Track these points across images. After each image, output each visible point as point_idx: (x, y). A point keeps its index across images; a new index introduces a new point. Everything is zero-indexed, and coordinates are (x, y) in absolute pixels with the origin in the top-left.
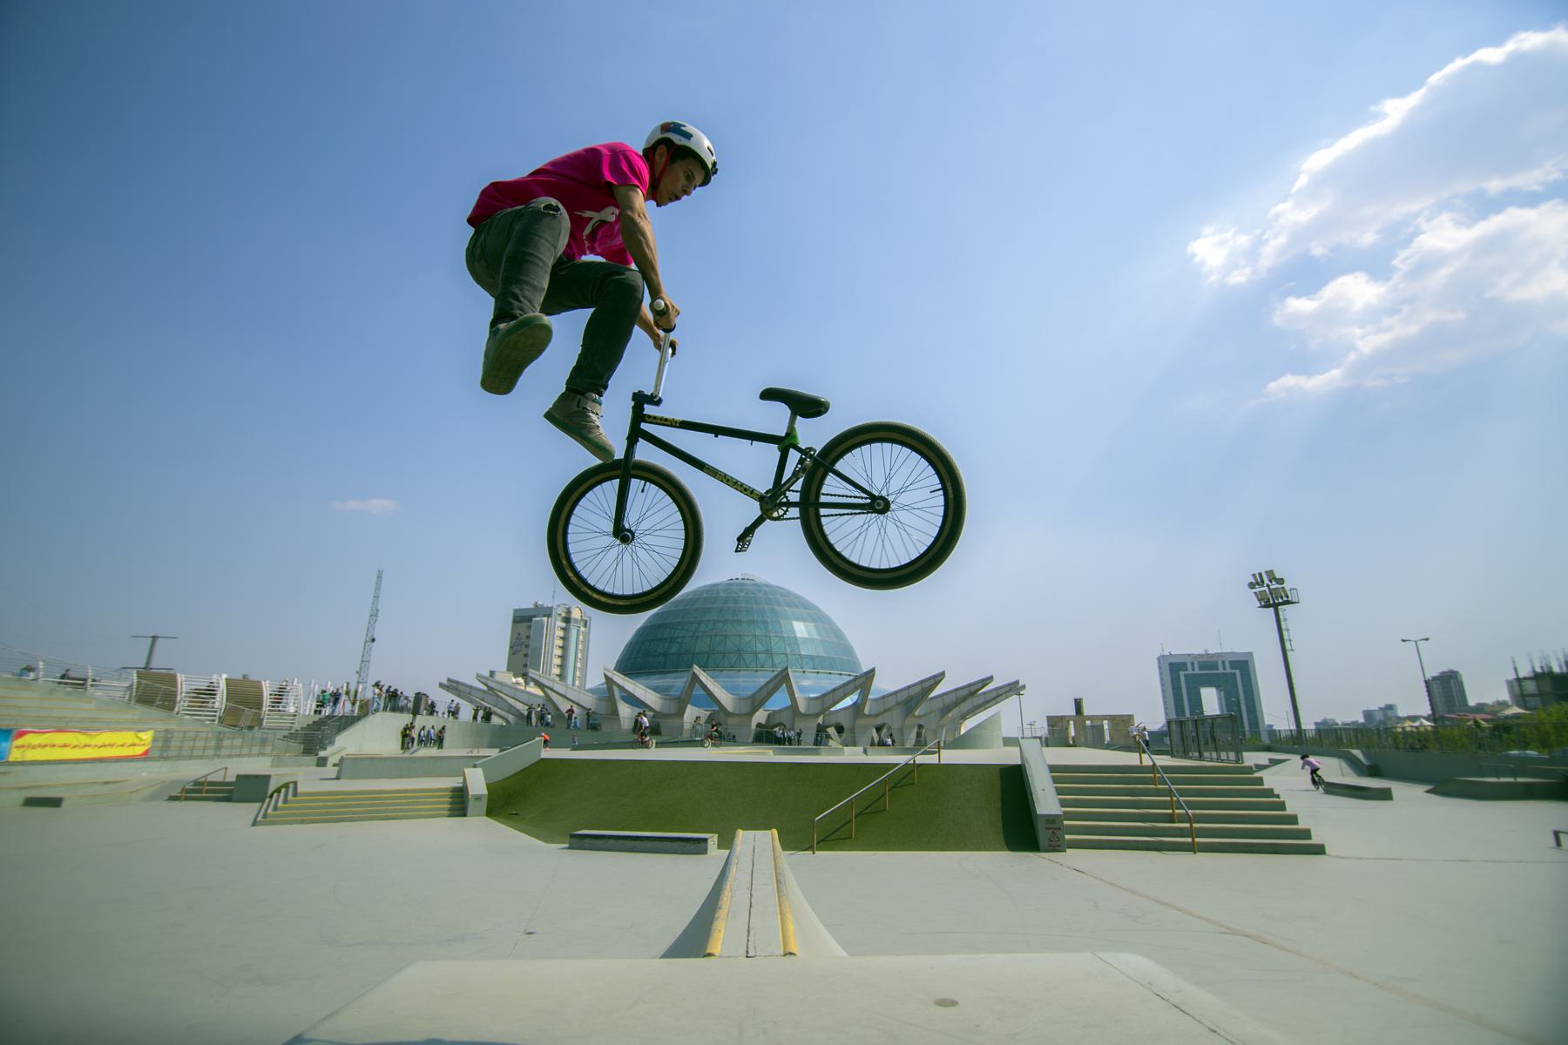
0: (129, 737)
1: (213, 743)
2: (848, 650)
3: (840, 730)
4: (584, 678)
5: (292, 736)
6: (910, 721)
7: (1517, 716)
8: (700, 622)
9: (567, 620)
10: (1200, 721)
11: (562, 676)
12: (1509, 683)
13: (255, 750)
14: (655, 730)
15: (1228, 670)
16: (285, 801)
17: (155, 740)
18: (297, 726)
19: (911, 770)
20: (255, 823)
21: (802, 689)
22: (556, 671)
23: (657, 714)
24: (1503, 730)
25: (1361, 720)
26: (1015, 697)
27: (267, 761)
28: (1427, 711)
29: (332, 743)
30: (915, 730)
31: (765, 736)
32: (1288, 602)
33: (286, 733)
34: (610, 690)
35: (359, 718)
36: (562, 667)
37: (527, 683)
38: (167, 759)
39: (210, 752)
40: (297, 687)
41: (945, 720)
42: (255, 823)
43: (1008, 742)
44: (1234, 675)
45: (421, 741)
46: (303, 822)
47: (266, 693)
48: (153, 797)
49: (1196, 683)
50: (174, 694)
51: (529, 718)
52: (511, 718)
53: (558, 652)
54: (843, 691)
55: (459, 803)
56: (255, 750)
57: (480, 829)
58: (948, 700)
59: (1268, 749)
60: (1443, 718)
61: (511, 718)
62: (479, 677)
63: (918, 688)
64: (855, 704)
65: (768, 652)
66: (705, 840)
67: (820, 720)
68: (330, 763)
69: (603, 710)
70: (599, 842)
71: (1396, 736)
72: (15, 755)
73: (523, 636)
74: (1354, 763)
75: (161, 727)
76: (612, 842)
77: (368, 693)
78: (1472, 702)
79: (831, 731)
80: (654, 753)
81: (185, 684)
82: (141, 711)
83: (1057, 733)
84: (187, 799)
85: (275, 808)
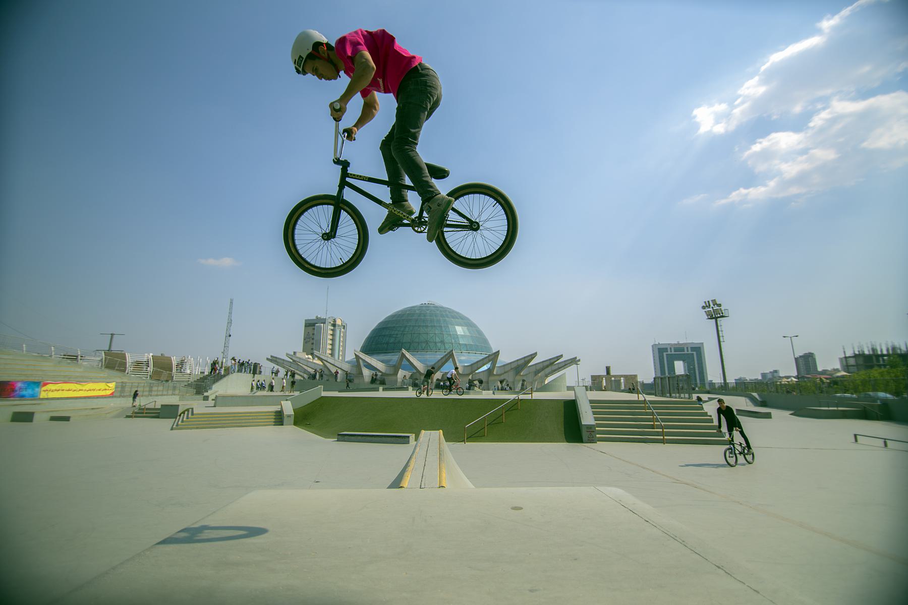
0: (102, 386)
1: (147, 389)
2: (485, 341)
3: (481, 382)
4: (344, 356)
6: (518, 378)
7: (843, 376)
9: (334, 325)
10: (674, 378)
11: (332, 355)
12: (841, 359)
13: (170, 392)
14: (383, 383)
16: (188, 418)
17: (116, 387)
18: (191, 380)
19: (516, 402)
20: (172, 429)
21: (461, 361)
22: (329, 352)
23: (383, 374)
24: (835, 383)
25: (760, 378)
27: (177, 398)
28: (795, 374)
29: (210, 389)
32: (723, 317)
34: (358, 361)
35: (225, 376)
36: (332, 350)
38: (123, 397)
39: (147, 393)
40: (190, 360)
42: (172, 429)
43: (570, 388)
44: (693, 355)
45: (258, 388)
47: (174, 363)
48: (118, 416)
49: (672, 359)
50: (125, 364)
51: (314, 377)
52: (305, 376)
55: (279, 418)
56: (170, 392)
57: (289, 431)
58: (538, 367)
59: (708, 392)
60: (803, 377)
61: (305, 376)
62: (287, 355)
63: (523, 361)
65: (442, 342)
67: (470, 377)
68: (210, 399)
69: (354, 372)
72: (43, 395)
74: (753, 400)
75: (120, 381)
77: (229, 363)
78: (820, 369)
79: (476, 382)
80: (381, 393)
81: (130, 359)
82: (107, 373)
83: (596, 383)
85: (183, 421)
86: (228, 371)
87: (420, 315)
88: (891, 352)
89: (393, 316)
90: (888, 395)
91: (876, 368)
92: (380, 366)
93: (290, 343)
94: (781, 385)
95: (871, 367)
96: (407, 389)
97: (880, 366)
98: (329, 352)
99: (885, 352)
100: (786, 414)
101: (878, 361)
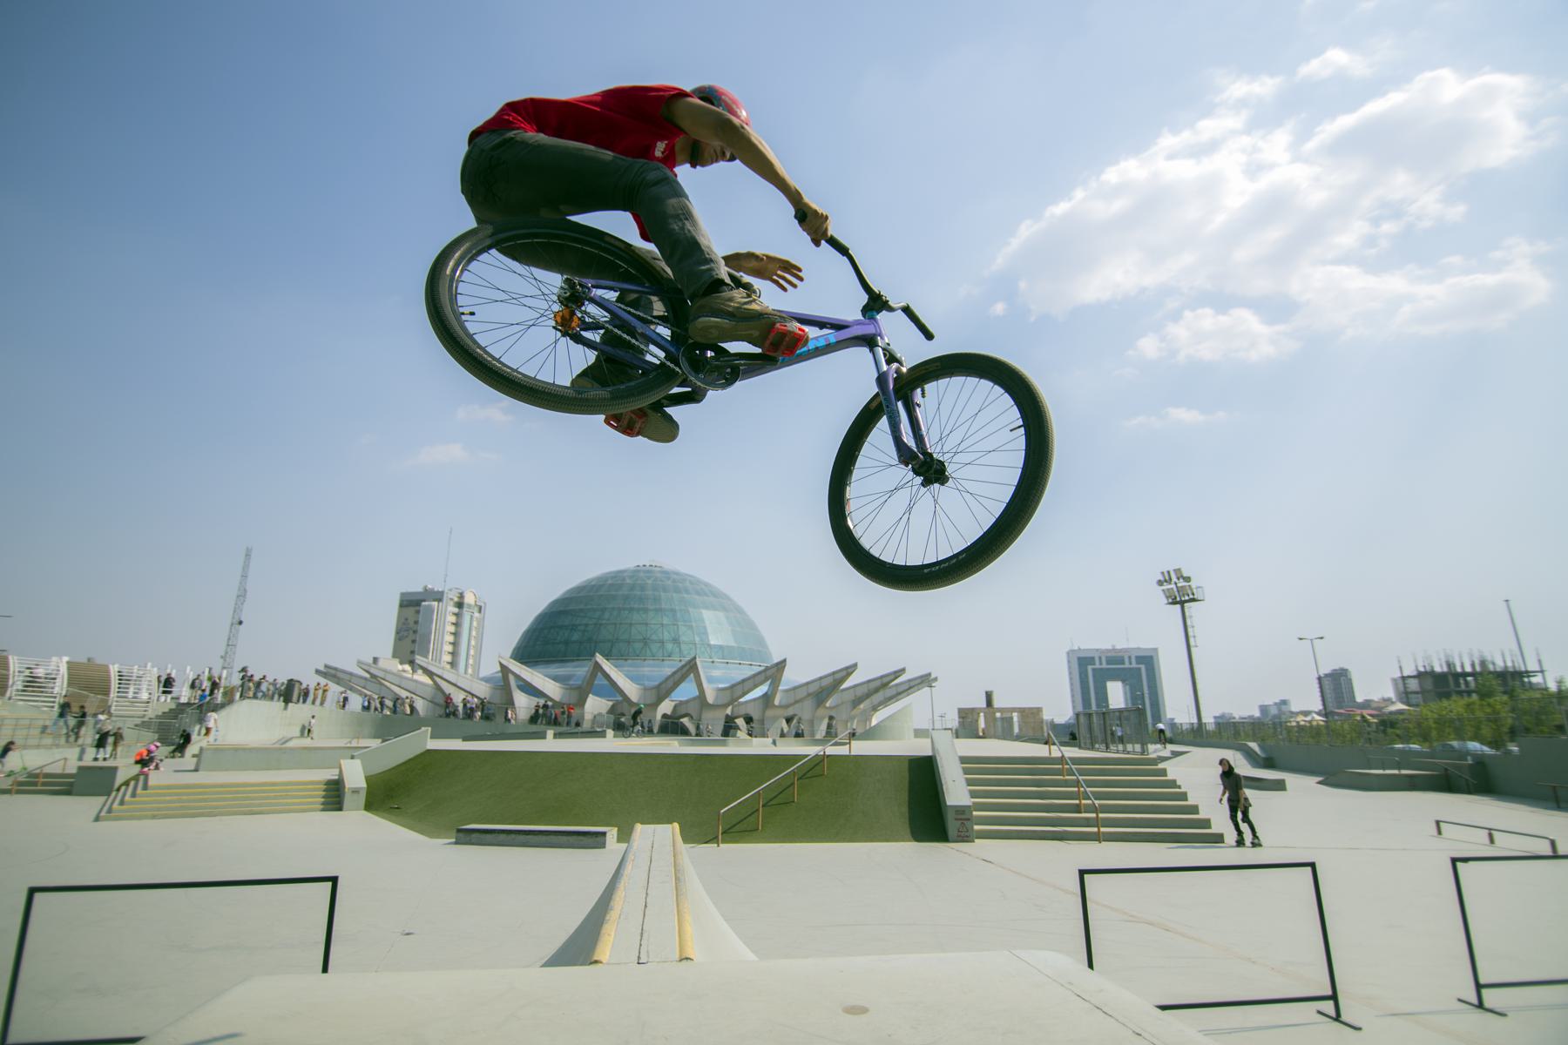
2: (761, 641)
3: (749, 720)
5: (145, 725)
6: (821, 711)
7: (1400, 712)
8: (603, 610)
9: (460, 605)
10: (1105, 714)
11: (453, 664)
12: (1394, 680)
14: (555, 722)
15: (1134, 665)
16: (134, 795)
18: (151, 714)
19: (820, 760)
20: (97, 819)
21: (711, 680)
22: (448, 658)
24: (1388, 724)
25: (1257, 714)
26: (927, 689)
28: (1319, 706)
30: (826, 721)
31: (671, 727)
33: (138, 721)
35: (223, 706)
36: (454, 654)
37: (414, 671)
41: (855, 712)
42: (97, 819)
43: (919, 733)
44: (1140, 671)
46: (154, 817)
49: (1103, 677)
53: (451, 638)
54: (754, 681)
55: (334, 796)
57: (357, 823)
60: (1333, 713)
62: (360, 663)
63: (830, 680)
64: (765, 695)
65: (676, 641)
66: (604, 834)
69: (497, 700)
70: (488, 837)
71: (1289, 730)
73: (411, 622)
76: (503, 837)
78: (1359, 699)
79: (740, 722)
80: (551, 743)
83: (967, 725)
84: (18, 792)
85: (122, 803)
86: (229, 700)
87: (632, 588)
88: (1478, 669)
89: (579, 589)
90: (1485, 748)
91: (1454, 697)
92: (553, 689)
93: (368, 640)
94: (1299, 726)
95: (1447, 695)
96: (602, 735)
97: (1460, 693)
98: (448, 658)
99: (1468, 669)
100: (1310, 781)
101: (1458, 684)
